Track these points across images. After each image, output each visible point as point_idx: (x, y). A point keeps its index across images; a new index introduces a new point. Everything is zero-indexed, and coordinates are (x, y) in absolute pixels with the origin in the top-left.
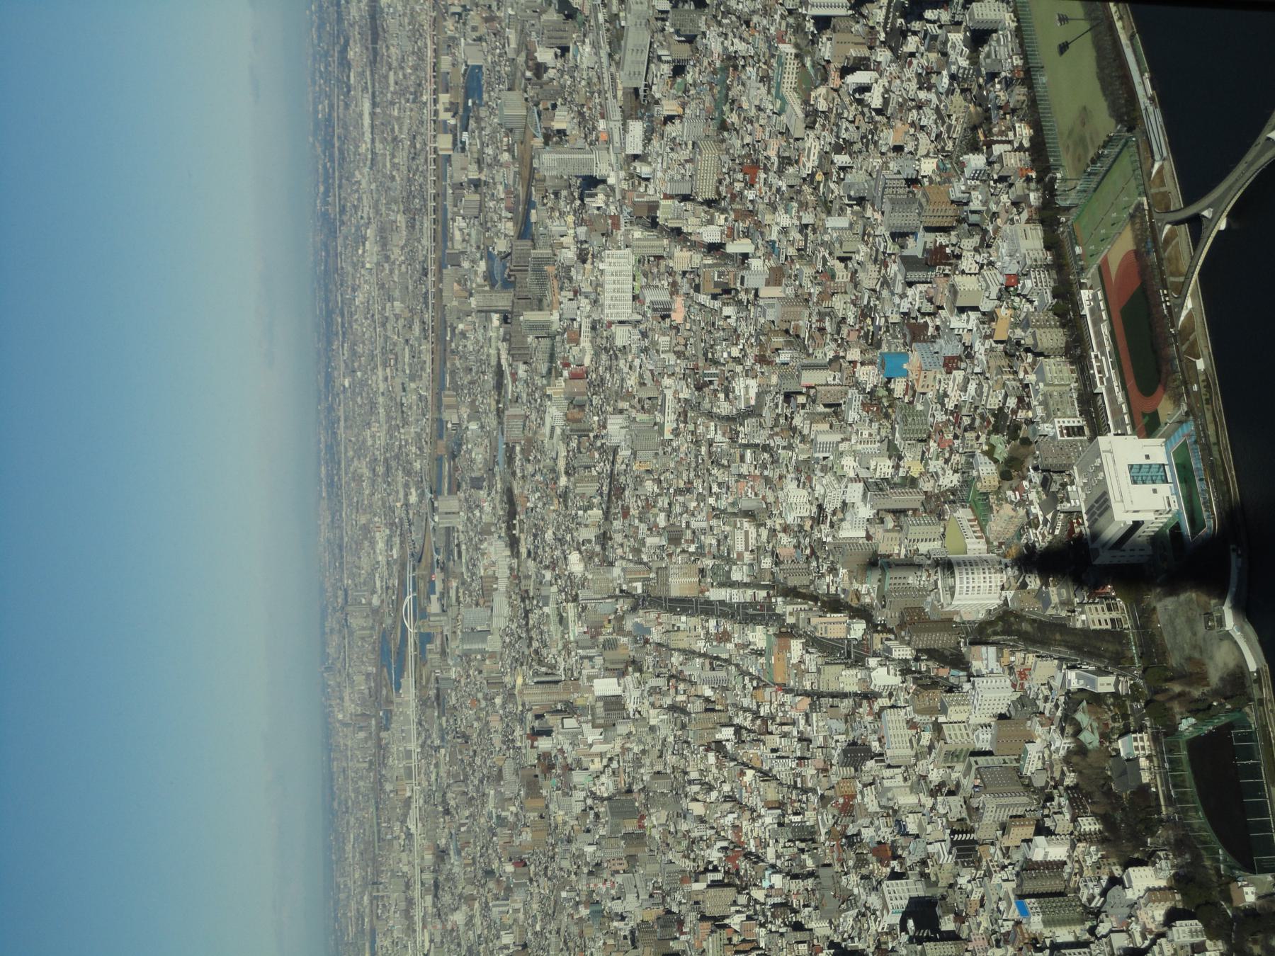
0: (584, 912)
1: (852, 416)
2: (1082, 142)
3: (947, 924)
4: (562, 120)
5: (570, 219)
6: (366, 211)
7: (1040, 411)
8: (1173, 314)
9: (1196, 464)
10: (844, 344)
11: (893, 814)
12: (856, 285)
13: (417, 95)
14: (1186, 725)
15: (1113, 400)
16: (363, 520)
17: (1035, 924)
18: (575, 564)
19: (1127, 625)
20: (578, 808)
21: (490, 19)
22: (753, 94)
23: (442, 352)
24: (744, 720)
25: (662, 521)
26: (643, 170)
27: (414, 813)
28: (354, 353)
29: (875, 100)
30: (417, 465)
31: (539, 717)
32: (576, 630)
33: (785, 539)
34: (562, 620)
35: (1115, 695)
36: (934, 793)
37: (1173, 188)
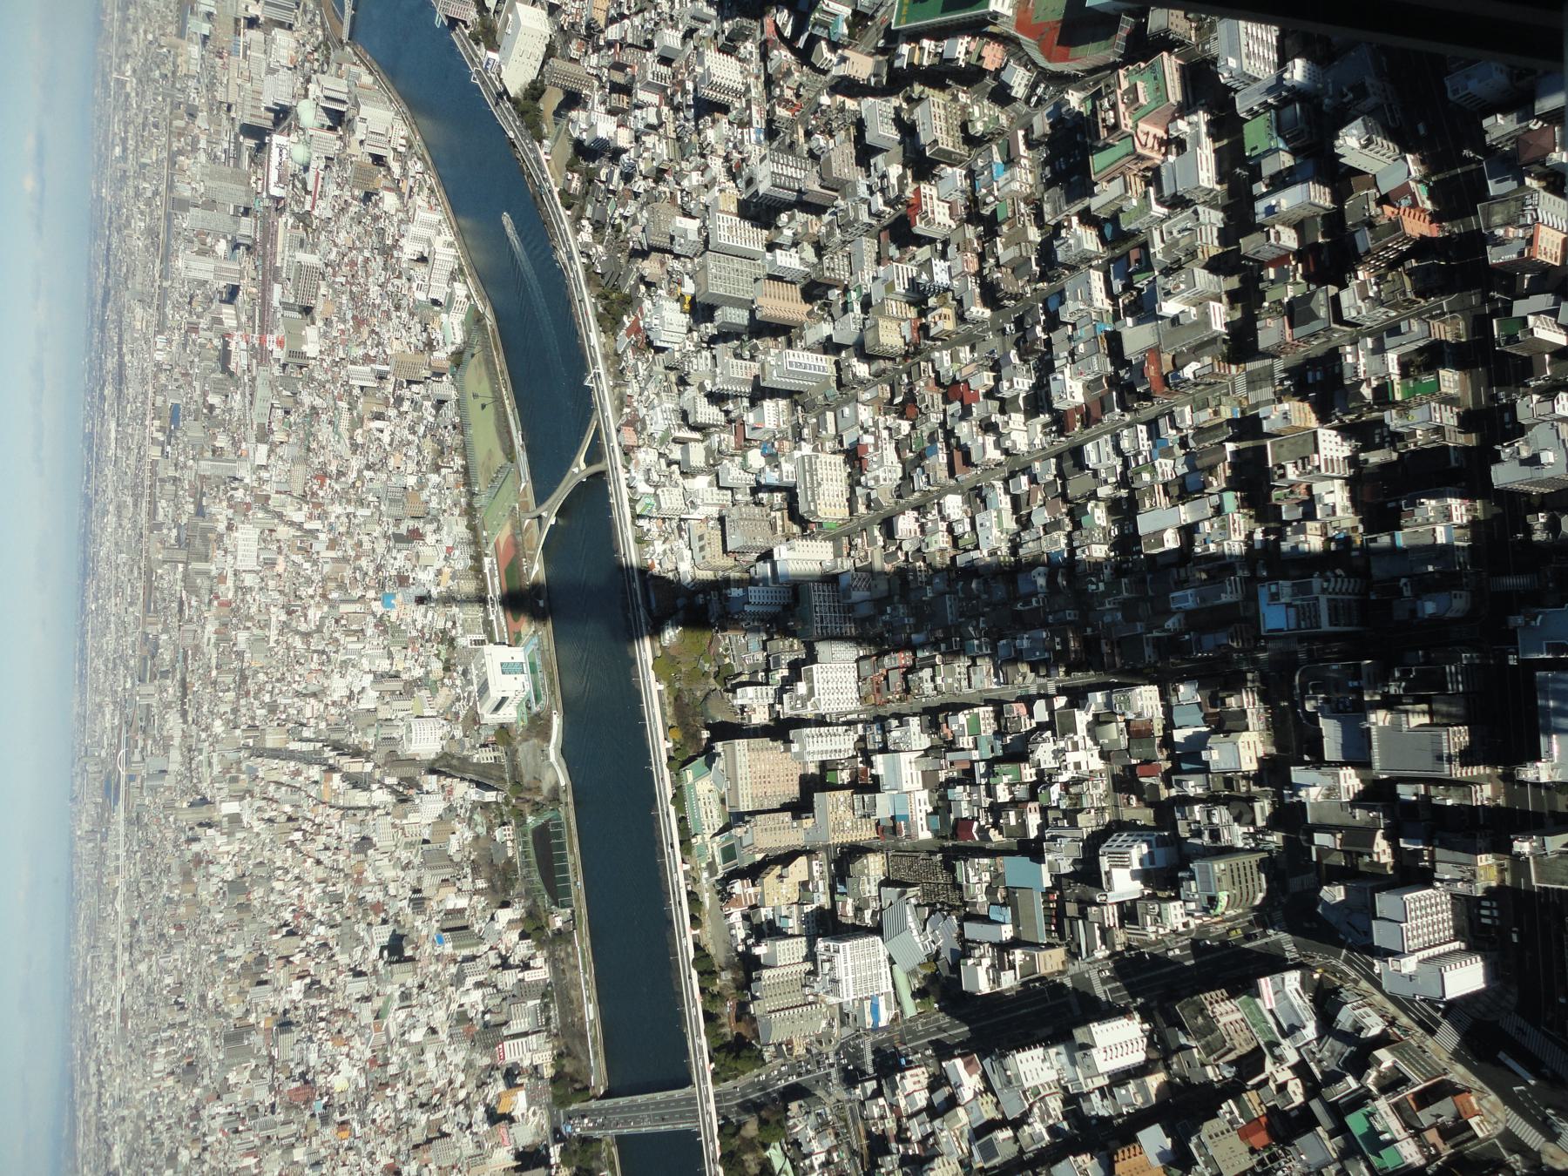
0: (214, 958)
1: (369, 632)
2: (488, 470)
3: (408, 952)
4: (222, 441)
5: (225, 504)
6: (110, 494)
7: (460, 630)
8: (528, 574)
9: (538, 662)
10: (367, 588)
11: (383, 885)
12: (374, 550)
13: (143, 421)
14: (530, 819)
15: (499, 624)
16: (98, 700)
17: (448, 948)
18: (218, 727)
19: (504, 761)
20: (213, 890)
21: (186, 375)
22: (324, 432)
23: (150, 588)
24: (307, 826)
25: (267, 698)
26: (265, 475)
27: (120, 898)
28: (98, 587)
29: (386, 438)
30: (132, 663)
31: (191, 829)
32: (217, 769)
33: (333, 710)
34: (210, 764)
35: (496, 803)
36: (403, 869)
37: (531, 498)
